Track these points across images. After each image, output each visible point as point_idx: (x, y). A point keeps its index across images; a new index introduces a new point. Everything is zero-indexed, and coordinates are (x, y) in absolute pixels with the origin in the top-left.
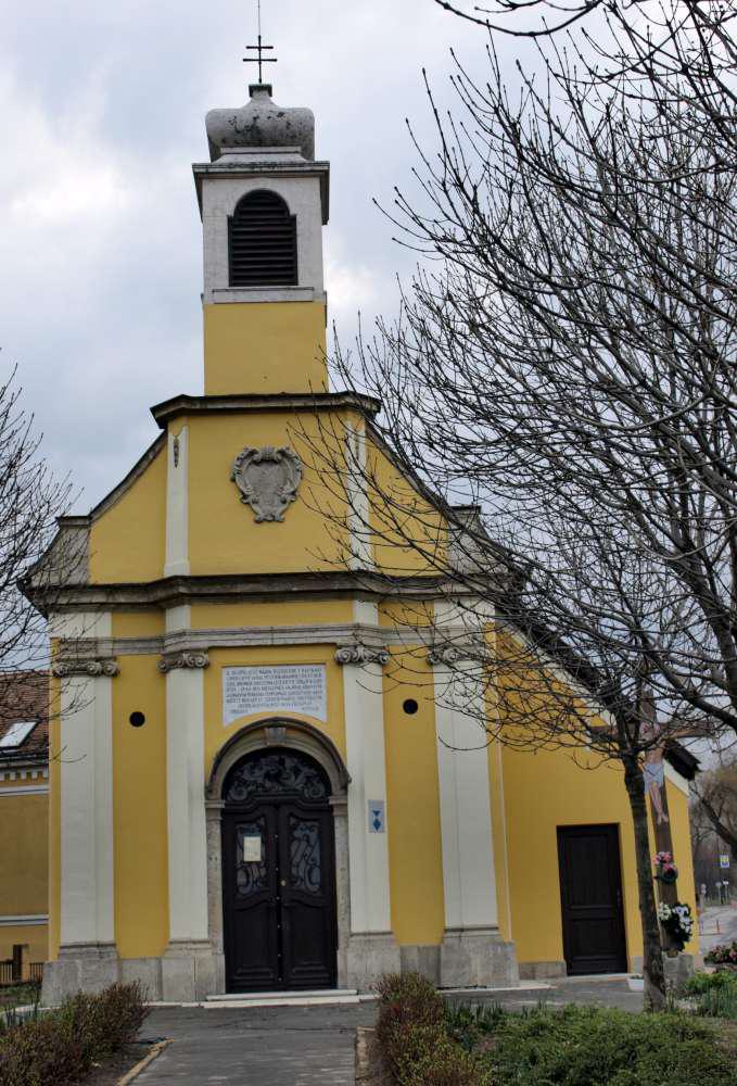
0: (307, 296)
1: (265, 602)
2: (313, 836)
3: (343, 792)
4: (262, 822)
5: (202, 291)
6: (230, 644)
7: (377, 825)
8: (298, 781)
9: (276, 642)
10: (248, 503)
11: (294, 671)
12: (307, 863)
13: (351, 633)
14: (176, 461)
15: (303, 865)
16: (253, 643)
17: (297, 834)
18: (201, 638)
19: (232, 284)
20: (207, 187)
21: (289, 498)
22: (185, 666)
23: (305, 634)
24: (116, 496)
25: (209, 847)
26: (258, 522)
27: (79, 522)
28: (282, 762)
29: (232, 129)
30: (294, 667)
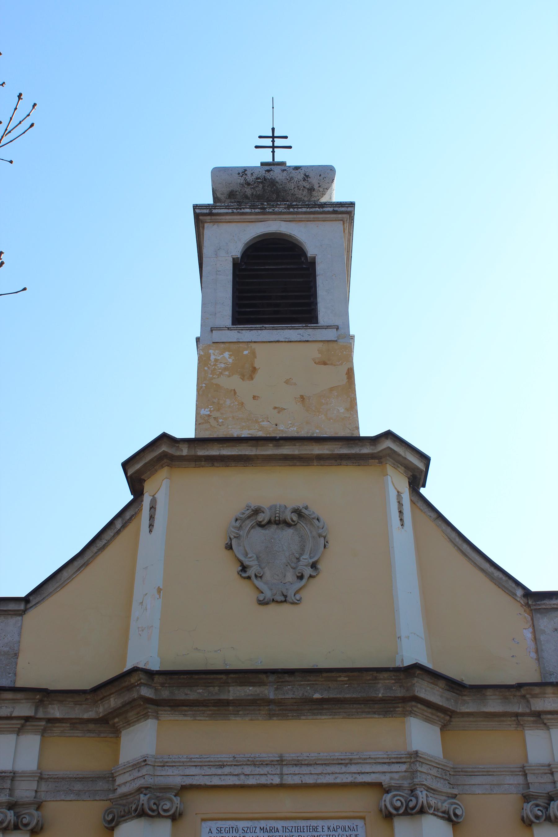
0: (331, 334)
1: (271, 716)
5: (199, 335)
6: (216, 781)
9: (289, 780)
10: (249, 578)
13: (403, 767)
14: (151, 526)
16: (251, 781)
18: (170, 771)
19: (233, 324)
20: (210, 230)
21: (308, 571)
22: (142, 814)
23: (330, 769)
24: (65, 574)
26: (263, 603)
27: (12, 606)
29: (242, 180)
30: (314, 823)
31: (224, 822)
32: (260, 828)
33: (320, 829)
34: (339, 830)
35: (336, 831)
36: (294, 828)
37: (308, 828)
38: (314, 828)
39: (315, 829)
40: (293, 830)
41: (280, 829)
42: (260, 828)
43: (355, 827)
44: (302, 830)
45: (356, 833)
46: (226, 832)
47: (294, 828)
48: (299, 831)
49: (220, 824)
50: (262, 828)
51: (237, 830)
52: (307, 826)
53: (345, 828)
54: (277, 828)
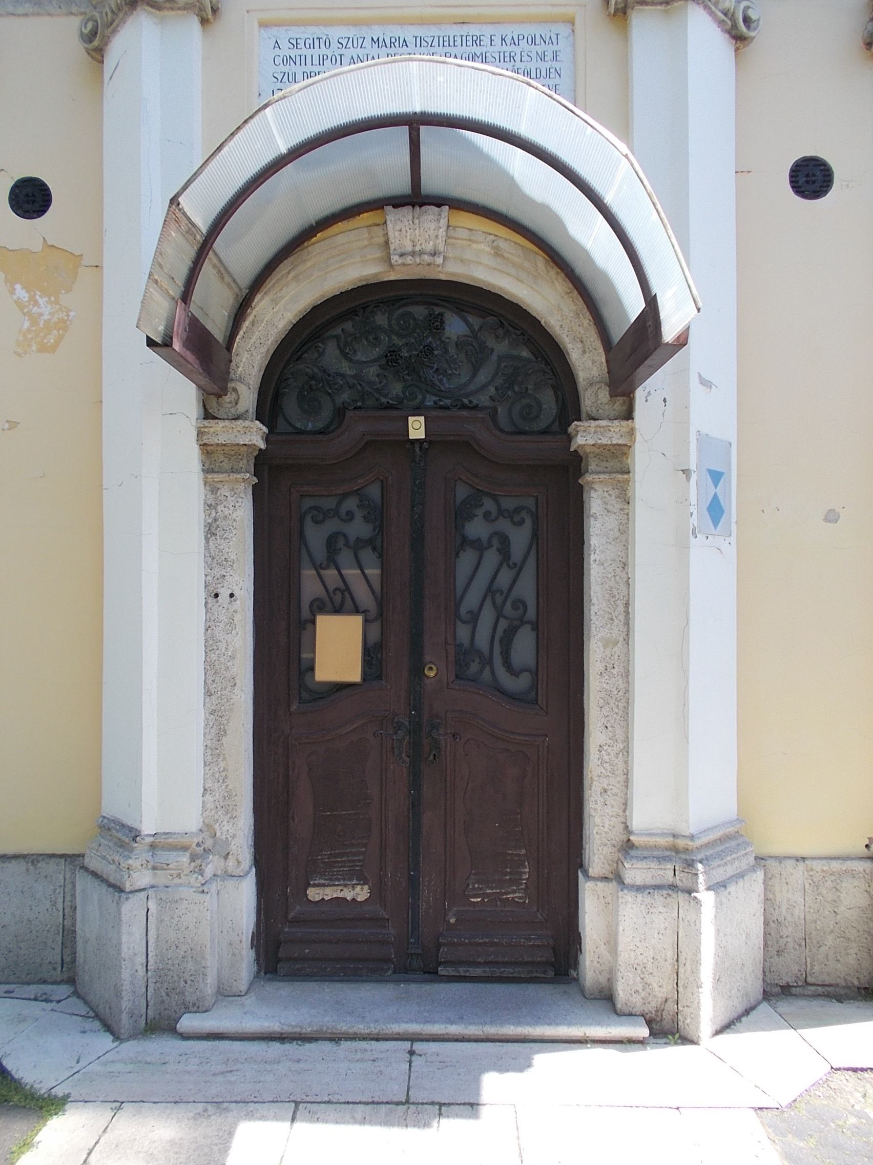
2: (520, 538)
3: (619, 405)
4: (374, 491)
7: (716, 510)
8: (482, 377)
11: (477, 41)
12: (500, 615)
15: (487, 617)
17: (477, 528)
25: (214, 560)
28: (436, 324)
30: (474, 30)
31: (302, 29)
32: (372, 39)
33: (486, 41)
34: (523, 43)
35: (517, 43)
36: (436, 39)
37: (464, 38)
38: (475, 38)
39: (477, 41)
40: (435, 43)
41: (410, 40)
42: (372, 39)
43: (554, 38)
44: (452, 44)
45: (555, 48)
46: (307, 46)
47: (436, 39)
48: (446, 44)
49: (294, 32)
50: (375, 39)
51: (327, 44)
52: (462, 36)
53: (534, 40)
54: (404, 40)
